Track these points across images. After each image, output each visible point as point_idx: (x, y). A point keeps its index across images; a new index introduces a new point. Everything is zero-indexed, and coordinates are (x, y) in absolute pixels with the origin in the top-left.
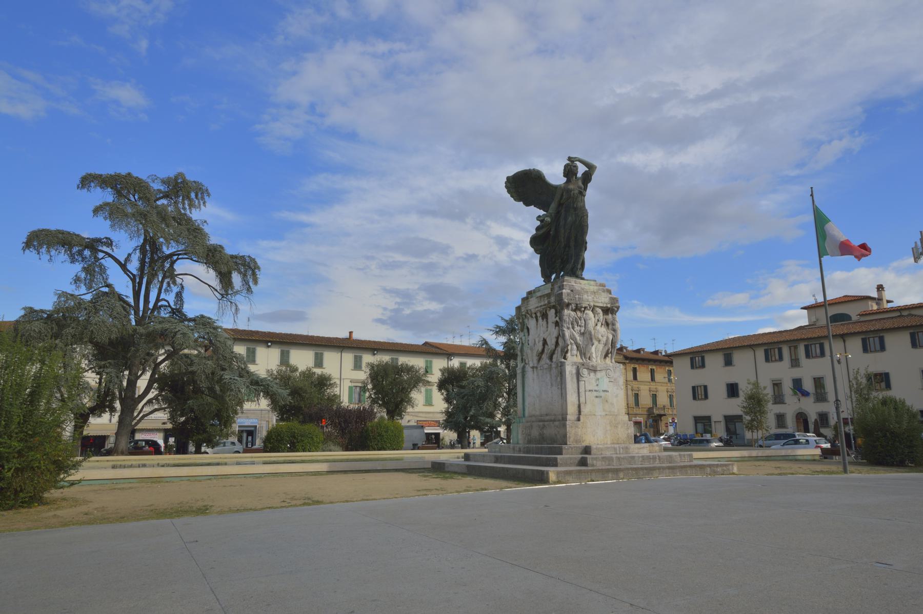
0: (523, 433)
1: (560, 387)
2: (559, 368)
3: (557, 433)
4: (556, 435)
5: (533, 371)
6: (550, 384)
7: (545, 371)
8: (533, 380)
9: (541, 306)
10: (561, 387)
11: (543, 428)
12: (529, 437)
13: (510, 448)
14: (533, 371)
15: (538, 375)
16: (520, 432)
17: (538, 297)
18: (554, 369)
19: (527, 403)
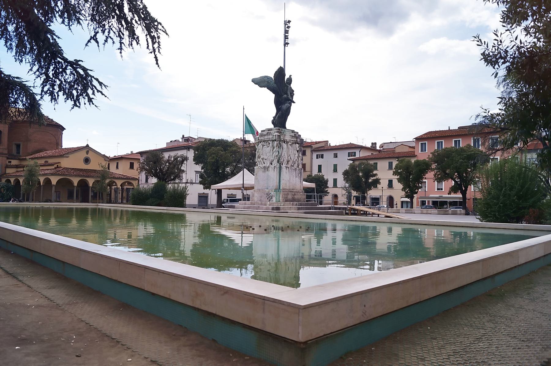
1: (300, 178)
4: (301, 198)
6: (295, 176)
7: (293, 170)
9: (292, 140)
11: (294, 195)
12: (286, 199)
13: (290, 204)
15: (289, 171)
16: (281, 196)
19: (281, 183)
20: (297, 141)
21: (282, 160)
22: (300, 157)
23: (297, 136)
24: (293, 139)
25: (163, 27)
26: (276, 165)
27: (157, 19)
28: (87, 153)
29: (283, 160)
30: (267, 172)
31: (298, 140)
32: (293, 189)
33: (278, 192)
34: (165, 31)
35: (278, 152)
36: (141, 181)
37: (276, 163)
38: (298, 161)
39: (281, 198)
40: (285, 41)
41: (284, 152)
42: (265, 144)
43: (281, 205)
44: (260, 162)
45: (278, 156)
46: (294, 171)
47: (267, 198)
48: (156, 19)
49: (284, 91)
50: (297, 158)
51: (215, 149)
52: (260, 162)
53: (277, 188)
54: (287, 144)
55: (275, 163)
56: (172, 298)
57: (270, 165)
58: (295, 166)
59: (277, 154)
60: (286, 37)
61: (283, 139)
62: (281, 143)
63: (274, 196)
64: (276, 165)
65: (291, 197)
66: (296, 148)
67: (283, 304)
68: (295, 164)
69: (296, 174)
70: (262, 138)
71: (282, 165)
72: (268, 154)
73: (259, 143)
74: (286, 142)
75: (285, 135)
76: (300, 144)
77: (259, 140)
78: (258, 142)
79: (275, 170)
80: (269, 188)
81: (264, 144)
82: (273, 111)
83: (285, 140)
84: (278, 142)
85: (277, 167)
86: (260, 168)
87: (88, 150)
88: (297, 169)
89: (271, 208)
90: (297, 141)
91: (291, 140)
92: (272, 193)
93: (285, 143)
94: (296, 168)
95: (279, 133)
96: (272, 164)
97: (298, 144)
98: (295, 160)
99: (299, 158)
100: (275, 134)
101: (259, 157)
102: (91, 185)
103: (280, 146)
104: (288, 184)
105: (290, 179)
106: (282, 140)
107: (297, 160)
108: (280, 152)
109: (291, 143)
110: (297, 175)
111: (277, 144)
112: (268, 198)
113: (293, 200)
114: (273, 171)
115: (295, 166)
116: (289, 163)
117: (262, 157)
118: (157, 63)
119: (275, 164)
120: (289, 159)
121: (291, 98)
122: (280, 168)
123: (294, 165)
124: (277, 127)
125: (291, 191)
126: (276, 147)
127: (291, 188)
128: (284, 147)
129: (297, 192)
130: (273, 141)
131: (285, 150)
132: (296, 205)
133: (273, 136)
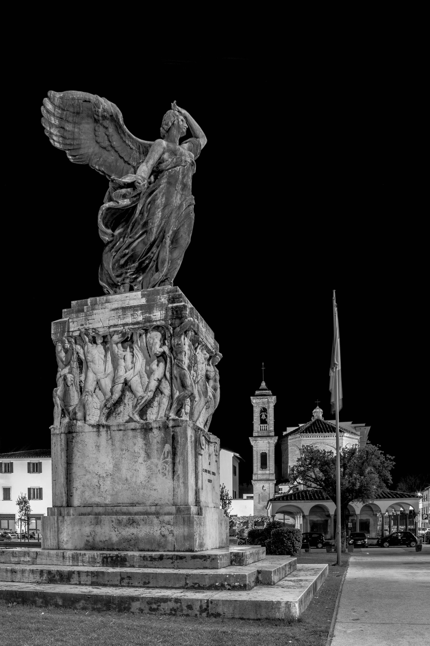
1: (169, 459)
3: (166, 533)
5: (99, 431)
6: (143, 454)
8: (98, 447)
10: (174, 459)
14: (99, 431)
19: (77, 484)
20: (148, 320)
32: (133, 505)
43: (22, 559)
46: (135, 437)
91: (115, 326)
105: (117, 467)
110: (155, 446)
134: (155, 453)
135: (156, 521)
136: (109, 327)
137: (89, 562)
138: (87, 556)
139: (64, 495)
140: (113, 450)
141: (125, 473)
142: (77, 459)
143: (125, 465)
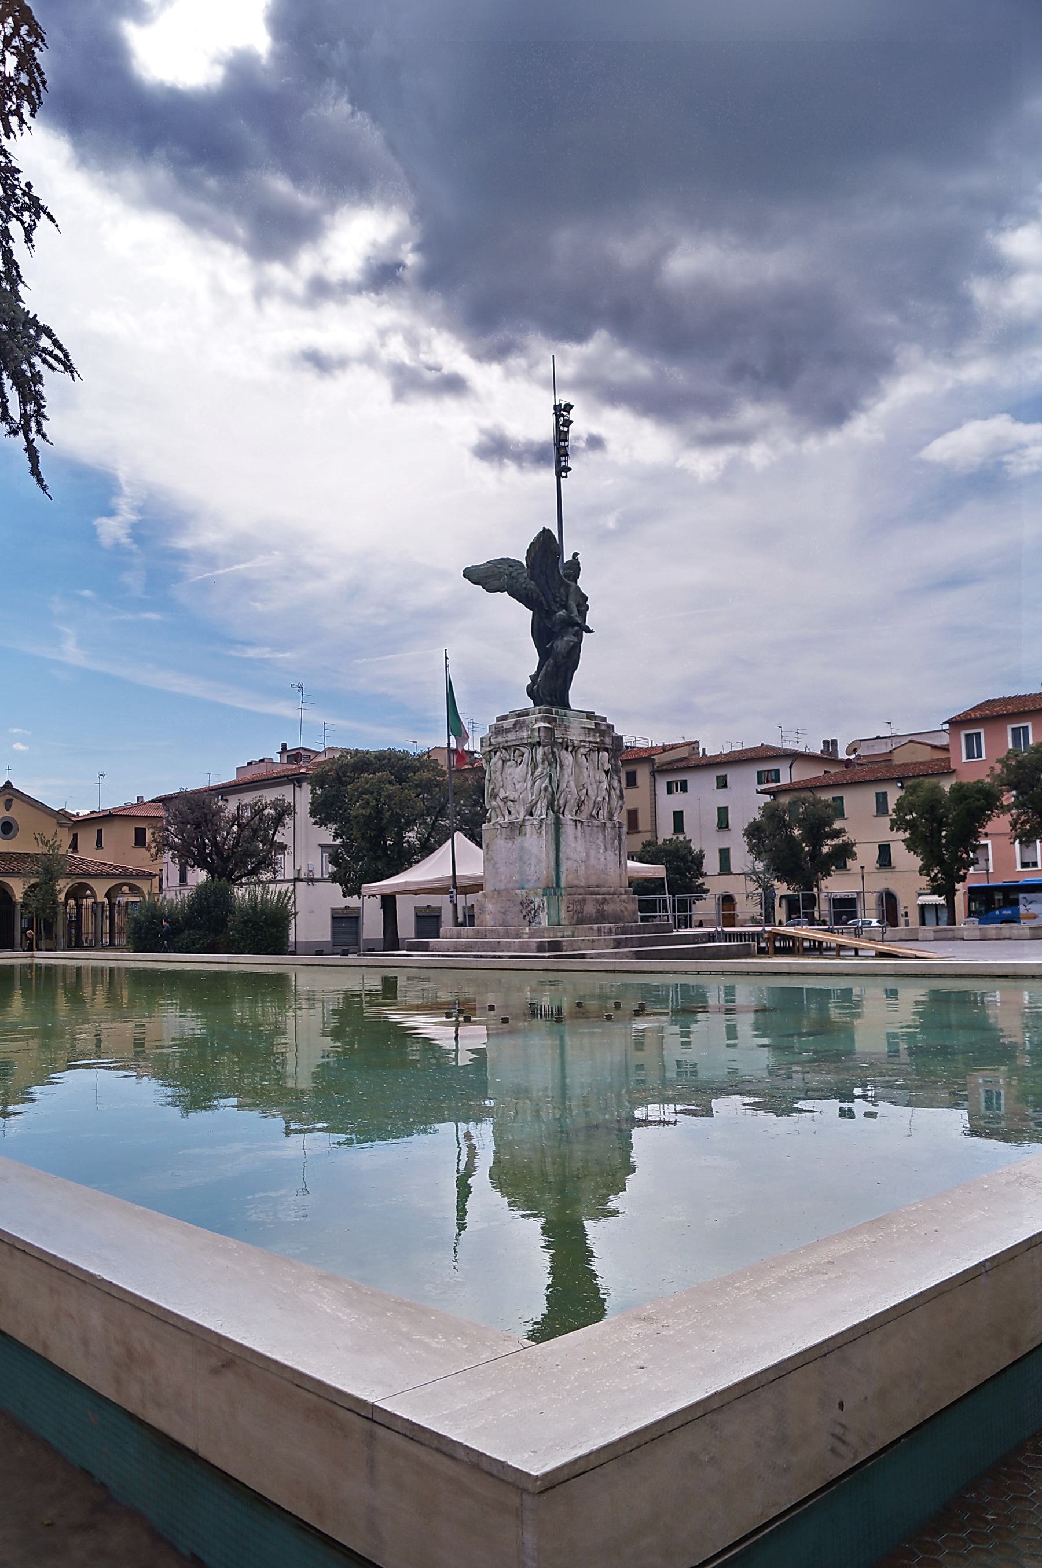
0: (570, 909)
1: (617, 852)
2: (617, 829)
3: (623, 909)
4: (622, 911)
5: (576, 825)
6: (603, 847)
7: (595, 829)
8: (576, 838)
9: (590, 742)
11: (603, 903)
12: (580, 915)
13: (592, 929)
14: (576, 825)
17: (584, 728)
18: (609, 829)
19: (563, 868)
20: (603, 742)
21: (561, 802)
22: (615, 790)
23: (603, 728)
24: (591, 739)
25: (56, 343)
26: (544, 816)
27: (36, 316)
28: (8, 805)
29: (566, 802)
30: (519, 839)
31: (608, 740)
32: (597, 886)
33: (555, 895)
34: (66, 355)
35: (548, 779)
36: (168, 879)
37: (544, 811)
38: (609, 803)
39: (563, 914)
40: (559, 462)
41: (566, 776)
42: (510, 756)
43: (565, 934)
44: (498, 810)
45: (550, 789)
46: (598, 832)
47: (522, 916)
48: (31, 316)
49: (558, 599)
50: (604, 793)
51: (372, 778)
52: (498, 810)
53: (550, 886)
54: (573, 753)
55: (541, 810)
56: (56, 1358)
57: (527, 817)
58: (603, 816)
59: (546, 783)
60: (562, 452)
61: (563, 739)
62: (555, 750)
63: (543, 909)
64: (544, 816)
65: (594, 910)
66: (603, 764)
67: (452, 1458)
68: (601, 811)
69: (605, 839)
70: (500, 739)
71: (561, 816)
72: (520, 784)
73: (493, 753)
74: (570, 749)
75: (568, 727)
76: (612, 750)
77: (490, 744)
78: (490, 752)
79: (544, 832)
80: (527, 886)
81: (508, 757)
82: (530, 660)
83: (567, 742)
84: (546, 748)
85: (549, 822)
86: (499, 827)
87: (9, 797)
88: (609, 824)
89: (535, 944)
90: (604, 744)
91: (584, 741)
92: (537, 900)
93: (567, 750)
94: (605, 823)
95: (549, 723)
96: (531, 814)
97: (608, 752)
98: (599, 799)
99: (612, 792)
100: (536, 726)
101: (494, 796)
102: (18, 896)
103: (553, 761)
104: (581, 872)
105: (587, 855)
106: (560, 741)
107: (607, 798)
108: (555, 778)
109: (587, 750)
111: (545, 754)
112: (525, 916)
113: (601, 917)
114: (535, 836)
115: (603, 816)
116: (582, 808)
117: (502, 794)
118: (35, 471)
119: (541, 815)
120: (583, 798)
121: (579, 620)
122: (558, 825)
123: (597, 814)
124: (541, 705)
125: (590, 891)
126: (543, 761)
127: (593, 881)
128: (566, 763)
129: (609, 894)
130: (533, 746)
131: (568, 771)
132: (610, 932)
133: (533, 730)
134: (609, 847)
135: (618, 900)
136: (581, 741)
137: (608, 933)
138: (607, 928)
139: (554, 877)
140: (585, 841)
141: (593, 861)
142: (563, 848)
143: (593, 853)
